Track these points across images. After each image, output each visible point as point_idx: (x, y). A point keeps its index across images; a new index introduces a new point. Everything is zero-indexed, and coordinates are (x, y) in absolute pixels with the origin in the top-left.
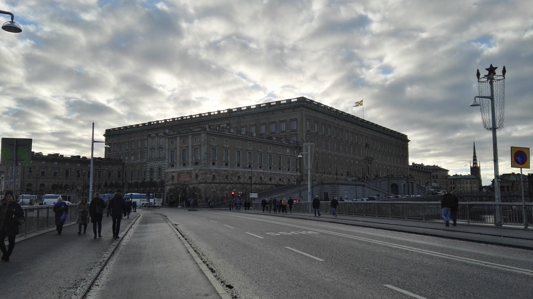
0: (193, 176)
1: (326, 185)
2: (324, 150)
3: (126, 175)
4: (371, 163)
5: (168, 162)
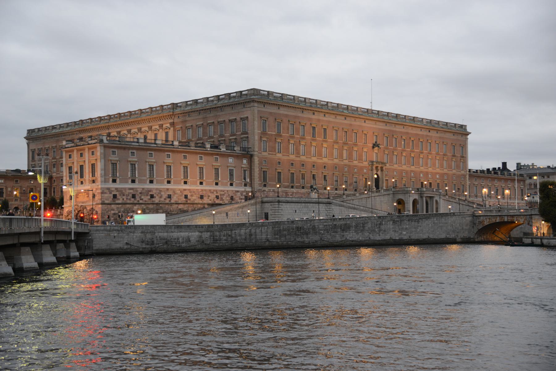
0: (91, 196)
1: (266, 204)
2: (292, 157)
3: (54, 192)
4: (382, 170)
5: (66, 179)
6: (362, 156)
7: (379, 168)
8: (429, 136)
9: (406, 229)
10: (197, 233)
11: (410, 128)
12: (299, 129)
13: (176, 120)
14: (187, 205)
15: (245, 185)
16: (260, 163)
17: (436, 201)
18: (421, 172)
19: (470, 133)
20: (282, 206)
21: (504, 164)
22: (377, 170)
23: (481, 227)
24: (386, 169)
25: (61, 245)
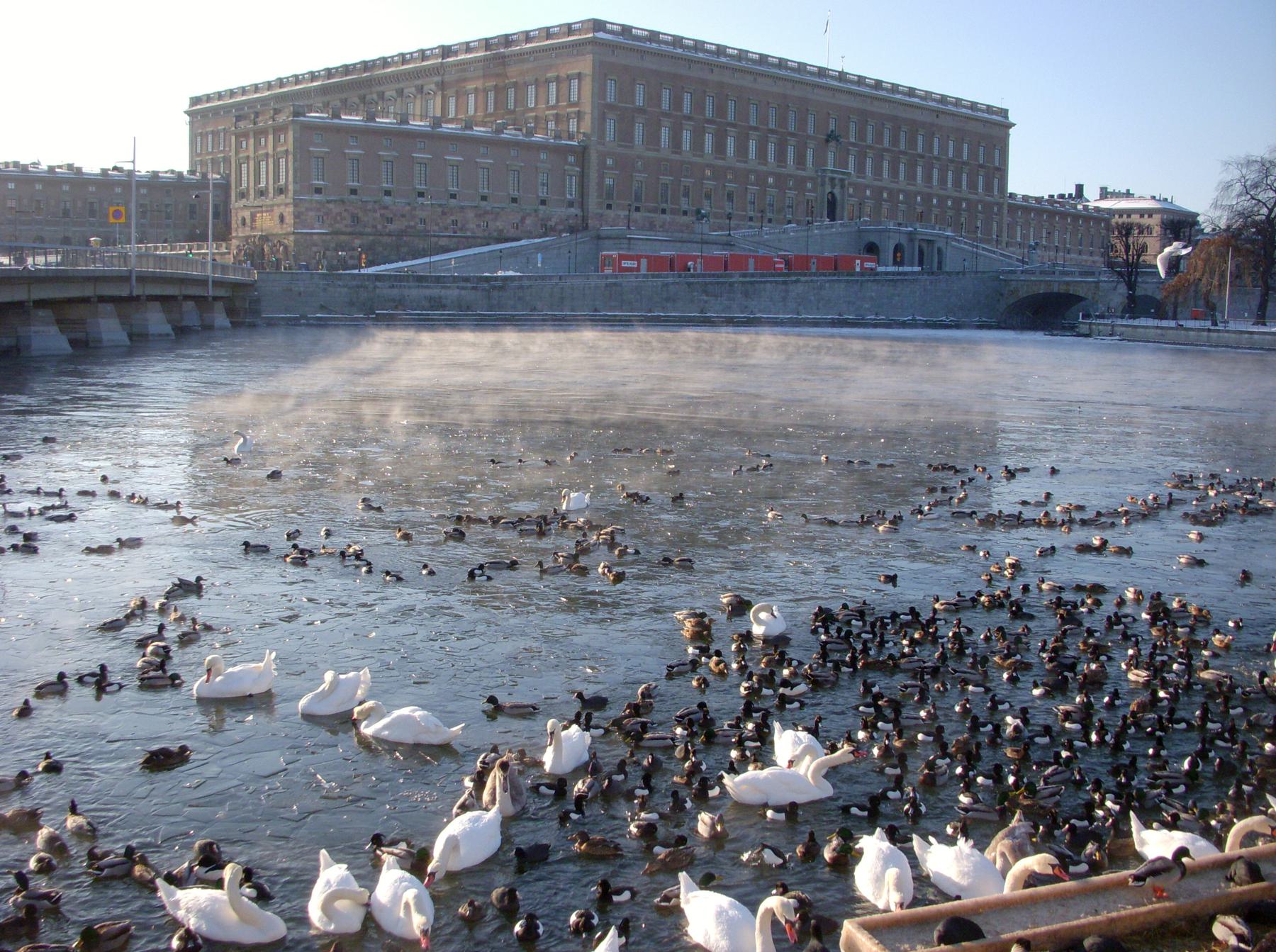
6: (805, 156)
9: (872, 298)
10: (456, 292)
12: (682, 100)
13: (447, 78)
14: (455, 240)
15: (571, 204)
16: (602, 164)
17: (939, 250)
18: (919, 193)
21: (1080, 188)
22: (833, 187)
23: (1011, 301)
24: (850, 184)
25: (189, 305)
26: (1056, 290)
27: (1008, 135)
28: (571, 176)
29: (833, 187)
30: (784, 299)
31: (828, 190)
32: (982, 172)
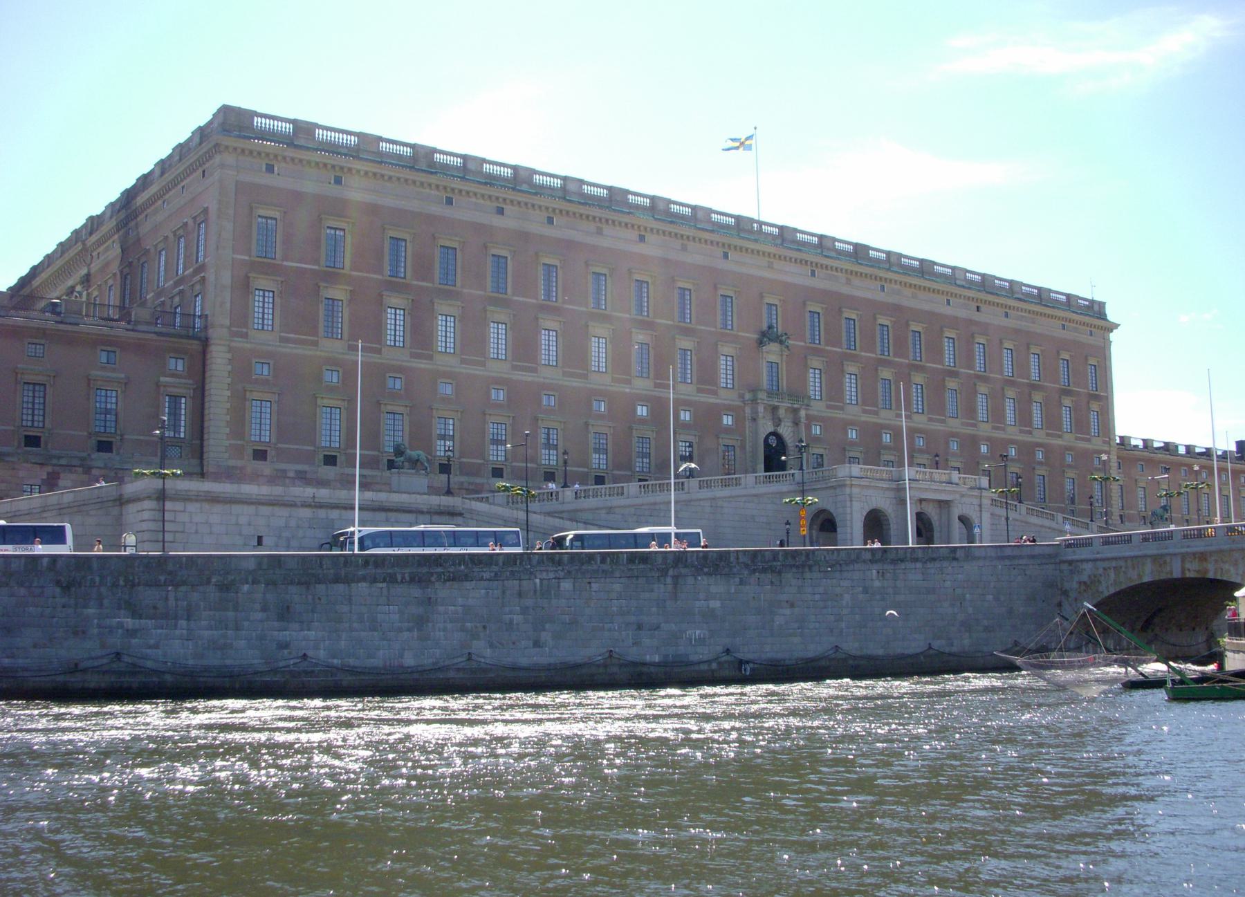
7: (782, 412)
8: (977, 323)
11: (908, 292)
17: (963, 520)
18: (953, 435)
19: (1116, 326)
20: (184, 518)
22: (778, 421)
26: (1177, 574)
27: (1107, 344)
28: (175, 399)
29: (778, 421)
30: (420, 622)
31: (766, 427)
32: (1067, 401)
